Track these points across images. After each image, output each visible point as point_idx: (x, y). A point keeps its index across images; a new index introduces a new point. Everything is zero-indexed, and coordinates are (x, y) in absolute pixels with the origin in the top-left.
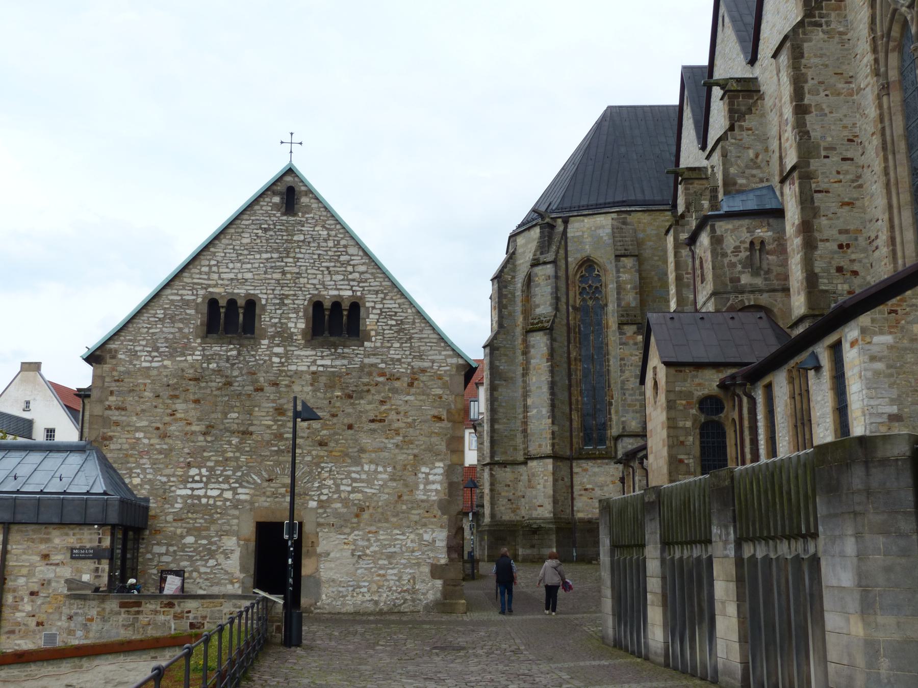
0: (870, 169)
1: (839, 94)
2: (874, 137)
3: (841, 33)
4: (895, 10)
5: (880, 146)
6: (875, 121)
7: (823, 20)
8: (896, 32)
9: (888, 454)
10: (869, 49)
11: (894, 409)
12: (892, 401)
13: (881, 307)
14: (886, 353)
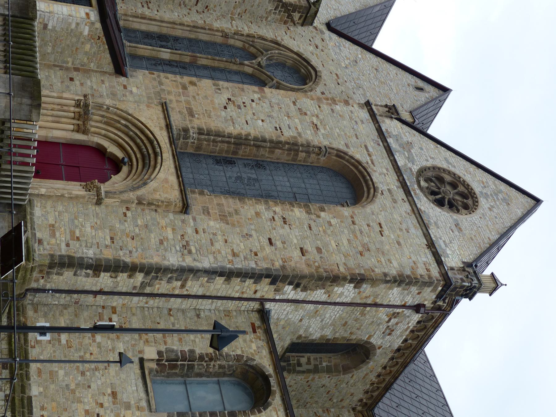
0: (187, 14)
1: (234, 8)
2: (203, 22)
3: (267, 18)
4: (262, 53)
5: (196, 25)
6: (211, 25)
7: (278, 12)
8: (252, 50)
9: (33, 114)
10: (250, 32)
11: (50, 27)
12: (54, 27)
13: (102, 33)
14: (79, 30)
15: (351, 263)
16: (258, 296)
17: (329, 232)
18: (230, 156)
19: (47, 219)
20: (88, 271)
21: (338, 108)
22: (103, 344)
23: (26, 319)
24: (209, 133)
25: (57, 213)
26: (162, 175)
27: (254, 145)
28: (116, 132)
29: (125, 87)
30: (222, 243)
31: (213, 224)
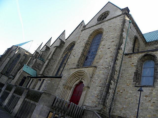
15: (118, 32)
16: (122, 54)
17: (108, 36)
18: (85, 57)
19: (90, 103)
20: (108, 95)
21: (81, 36)
22: (129, 96)
23: (117, 116)
24: (79, 60)
25: (89, 100)
26: (86, 71)
27: (84, 52)
28: (73, 81)
29: (64, 77)
30: (107, 59)
31: (101, 61)
